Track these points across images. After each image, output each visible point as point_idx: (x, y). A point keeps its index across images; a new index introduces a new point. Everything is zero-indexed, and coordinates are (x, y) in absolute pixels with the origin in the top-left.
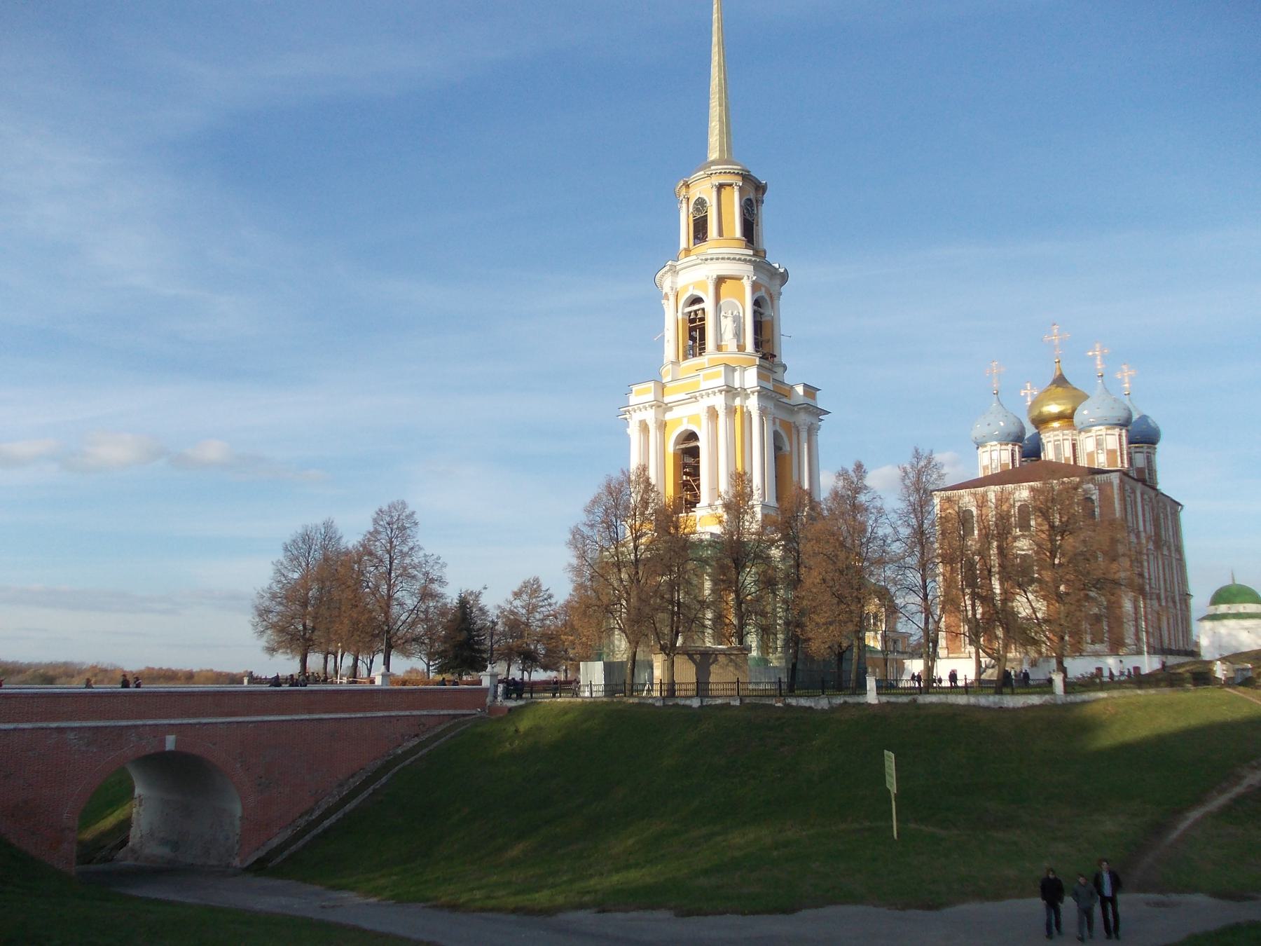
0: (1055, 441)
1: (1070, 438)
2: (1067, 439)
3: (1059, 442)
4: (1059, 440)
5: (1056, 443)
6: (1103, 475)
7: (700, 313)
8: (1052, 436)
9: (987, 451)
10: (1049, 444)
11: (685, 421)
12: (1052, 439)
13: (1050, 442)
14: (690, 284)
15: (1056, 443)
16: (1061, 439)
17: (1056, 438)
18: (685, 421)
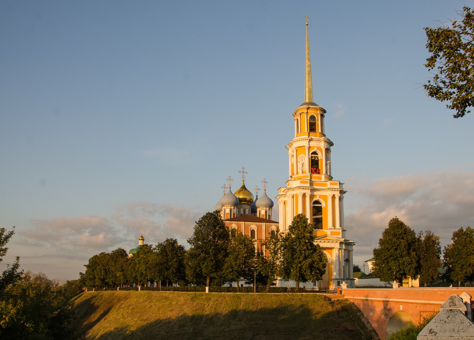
0: (244, 208)
1: (248, 208)
2: (248, 208)
4: (245, 208)
6: (277, 224)
7: (316, 159)
9: (229, 208)
10: (241, 209)
11: (318, 196)
12: (243, 207)
13: (242, 208)
14: (316, 147)
16: (246, 208)
17: (244, 207)
18: (318, 196)
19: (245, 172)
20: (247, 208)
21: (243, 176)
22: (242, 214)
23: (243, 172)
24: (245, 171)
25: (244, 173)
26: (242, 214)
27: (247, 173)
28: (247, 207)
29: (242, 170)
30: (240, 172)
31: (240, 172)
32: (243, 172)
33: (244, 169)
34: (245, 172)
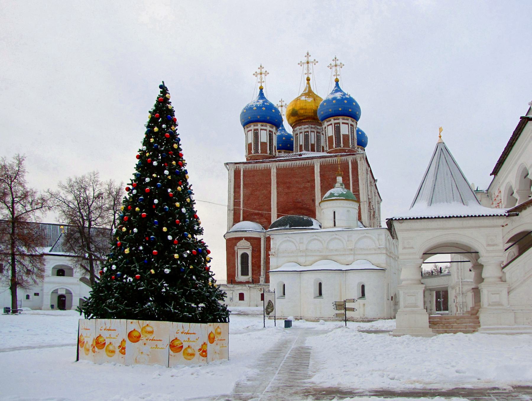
0: (305, 132)
2: (314, 132)
3: (308, 133)
4: (308, 132)
5: (305, 134)
8: (303, 128)
10: (301, 134)
12: (303, 131)
15: (305, 134)
16: (310, 131)
19: (312, 62)
20: (311, 131)
21: (308, 70)
22: (302, 145)
23: (308, 63)
24: (311, 59)
25: (310, 65)
26: (302, 145)
27: (315, 62)
28: (313, 130)
29: (304, 60)
30: (301, 64)
31: (301, 64)
32: (308, 63)
33: (310, 56)
34: (312, 62)
